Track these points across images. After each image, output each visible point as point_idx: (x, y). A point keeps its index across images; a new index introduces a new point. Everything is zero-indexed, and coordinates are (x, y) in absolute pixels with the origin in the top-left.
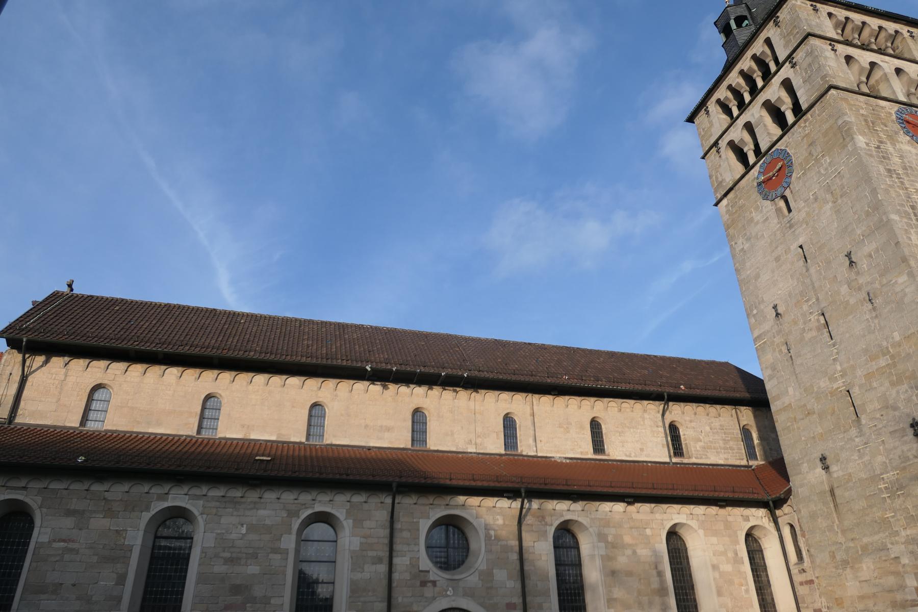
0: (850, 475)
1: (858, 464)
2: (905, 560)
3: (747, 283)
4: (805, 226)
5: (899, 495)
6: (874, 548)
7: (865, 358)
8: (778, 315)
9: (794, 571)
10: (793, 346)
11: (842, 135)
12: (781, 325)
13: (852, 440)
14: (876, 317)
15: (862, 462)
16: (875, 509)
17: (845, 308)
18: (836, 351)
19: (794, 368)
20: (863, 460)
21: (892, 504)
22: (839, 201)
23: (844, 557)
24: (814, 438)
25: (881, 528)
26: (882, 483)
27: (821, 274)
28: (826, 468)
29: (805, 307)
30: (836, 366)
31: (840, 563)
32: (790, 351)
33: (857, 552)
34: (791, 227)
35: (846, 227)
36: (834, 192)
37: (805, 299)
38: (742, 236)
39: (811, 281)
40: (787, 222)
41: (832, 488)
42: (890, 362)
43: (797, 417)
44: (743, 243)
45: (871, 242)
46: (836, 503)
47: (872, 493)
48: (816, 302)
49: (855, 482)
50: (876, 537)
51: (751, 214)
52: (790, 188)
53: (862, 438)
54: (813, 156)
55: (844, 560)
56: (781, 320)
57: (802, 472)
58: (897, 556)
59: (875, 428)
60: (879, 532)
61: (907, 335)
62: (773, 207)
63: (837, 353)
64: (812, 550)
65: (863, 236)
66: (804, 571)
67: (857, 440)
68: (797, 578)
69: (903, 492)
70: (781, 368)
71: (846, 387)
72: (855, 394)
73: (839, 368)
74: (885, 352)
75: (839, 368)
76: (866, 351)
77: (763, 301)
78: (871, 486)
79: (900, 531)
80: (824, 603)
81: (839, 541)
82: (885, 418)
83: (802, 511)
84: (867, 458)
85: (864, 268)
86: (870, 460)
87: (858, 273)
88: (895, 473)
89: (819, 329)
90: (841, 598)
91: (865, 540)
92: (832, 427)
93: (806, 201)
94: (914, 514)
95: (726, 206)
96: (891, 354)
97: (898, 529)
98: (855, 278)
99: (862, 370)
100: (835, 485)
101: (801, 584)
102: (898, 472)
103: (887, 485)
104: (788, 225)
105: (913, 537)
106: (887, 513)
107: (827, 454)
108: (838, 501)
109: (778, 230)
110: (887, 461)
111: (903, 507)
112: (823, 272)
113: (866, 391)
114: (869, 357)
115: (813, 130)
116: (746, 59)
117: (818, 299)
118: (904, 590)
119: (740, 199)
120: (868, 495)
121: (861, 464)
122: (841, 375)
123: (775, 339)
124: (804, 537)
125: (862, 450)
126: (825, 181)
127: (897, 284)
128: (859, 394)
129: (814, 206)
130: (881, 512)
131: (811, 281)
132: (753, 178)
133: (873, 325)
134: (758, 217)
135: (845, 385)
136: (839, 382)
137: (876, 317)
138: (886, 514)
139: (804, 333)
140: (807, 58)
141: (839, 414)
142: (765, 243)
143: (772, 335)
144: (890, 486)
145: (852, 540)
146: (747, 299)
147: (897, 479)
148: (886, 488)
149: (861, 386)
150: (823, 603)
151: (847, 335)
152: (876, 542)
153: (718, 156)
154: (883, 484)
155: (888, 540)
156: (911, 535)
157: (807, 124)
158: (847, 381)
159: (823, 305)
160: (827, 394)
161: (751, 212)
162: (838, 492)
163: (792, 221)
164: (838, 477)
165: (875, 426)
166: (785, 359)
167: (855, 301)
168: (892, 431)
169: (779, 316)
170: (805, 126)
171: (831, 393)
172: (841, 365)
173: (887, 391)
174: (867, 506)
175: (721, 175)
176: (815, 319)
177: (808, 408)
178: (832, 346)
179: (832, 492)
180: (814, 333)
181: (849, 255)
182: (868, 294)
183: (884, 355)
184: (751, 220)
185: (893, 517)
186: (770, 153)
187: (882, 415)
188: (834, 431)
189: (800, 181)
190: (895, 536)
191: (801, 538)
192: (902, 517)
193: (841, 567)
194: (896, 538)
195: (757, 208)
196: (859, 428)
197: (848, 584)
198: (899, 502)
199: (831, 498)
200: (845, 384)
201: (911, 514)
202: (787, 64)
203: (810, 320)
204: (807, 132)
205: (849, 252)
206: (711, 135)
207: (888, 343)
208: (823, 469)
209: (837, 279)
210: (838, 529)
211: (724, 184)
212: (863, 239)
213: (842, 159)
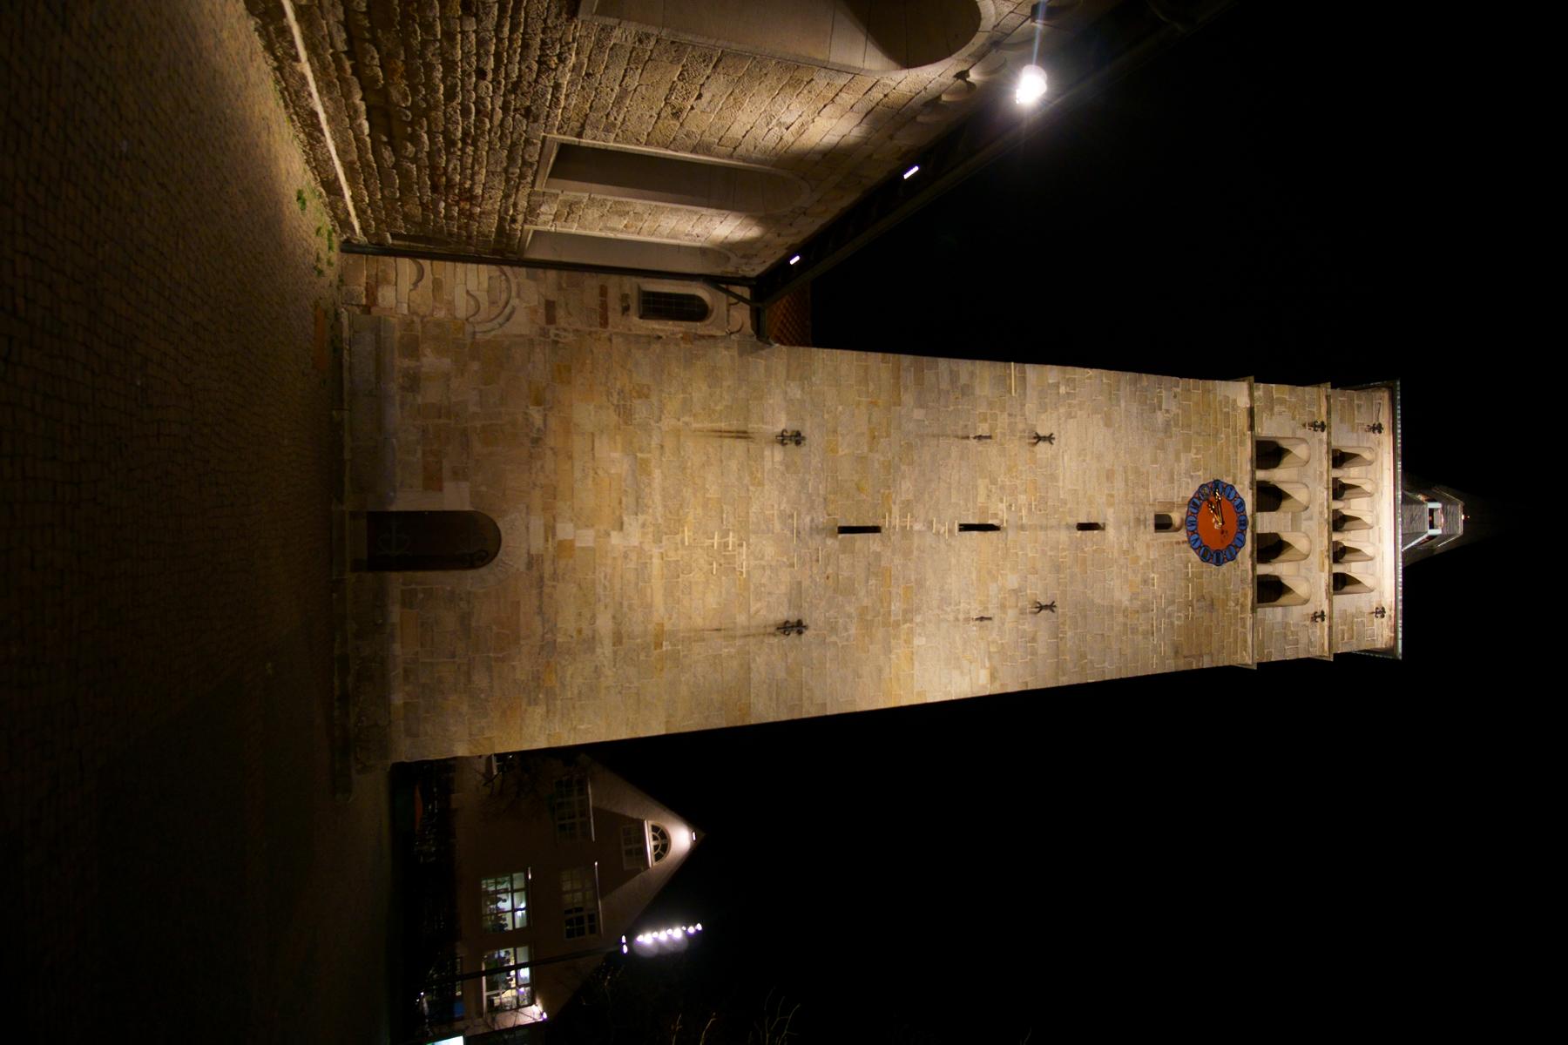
0: (761, 484)
1: (773, 506)
2: (616, 539)
3: (1110, 393)
5: (712, 564)
6: (643, 486)
7: (913, 578)
8: (1039, 438)
9: (630, 285)
10: (980, 449)
12: (1021, 438)
13: (812, 508)
14: (957, 619)
15: (773, 515)
16: (700, 511)
17: (989, 572)
18: (942, 531)
20: (776, 518)
21: (701, 547)
23: (637, 416)
24: (835, 431)
25: (670, 512)
26: (735, 540)
27: (1052, 549)
28: (783, 439)
30: (922, 524)
31: (628, 403)
32: (976, 440)
33: (641, 450)
34: (1138, 521)
35: (1085, 617)
37: (1033, 503)
38: (1178, 415)
39: (1052, 527)
41: (750, 438)
42: (892, 618)
43: (876, 409)
45: (1048, 649)
46: (725, 437)
47: (725, 516)
48: (1020, 523)
49: (748, 490)
50: (657, 498)
51: (1194, 451)
52: (1184, 542)
53: (807, 529)
55: (631, 415)
56: (1027, 441)
57: (788, 382)
58: (625, 527)
59: (814, 558)
60: (665, 506)
61: (915, 657)
62: (1180, 499)
63: (938, 533)
64: (657, 347)
65: (1062, 638)
66: (626, 310)
67: (808, 519)
68: (613, 281)
69: (714, 573)
70: (960, 407)
71: (887, 530)
72: (871, 542)
73: (917, 527)
74: (908, 614)
75: (917, 527)
76: (920, 583)
77: (1070, 416)
78: (735, 518)
79: (660, 547)
80: (565, 337)
81: (663, 417)
82: (823, 581)
83: (726, 353)
84: (777, 527)
85: (1024, 624)
86: (773, 533)
87: (1022, 612)
88: (744, 570)
89: (984, 510)
90: (569, 383)
91: (657, 473)
92: (840, 478)
93: (1153, 563)
94: (680, 580)
95: (1235, 401)
96: (901, 622)
97: (664, 542)
98: (1019, 605)
99: (899, 568)
100: (752, 446)
101: (603, 292)
102: (744, 576)
103: (730, 548)
104: (1142, 517)
105: (648, 566)
106: (691, 534)
107: (803, 449)
108: (727, 441)
109: (1148, 494)
110: (763, 563)
111: (694, 565)
112: (1052, 553)
113: (869, 564)
114: (912, 587)
117: (1022, 528)
118: (572, 520)
119: (1228, 437)
120: (725, 507)
121: (772, 512)
122: (906, 527)
123: (1006, 415)
124: (682, 338)
125: (790, 521)
126: (1157, 608)
127: (981, 668)
128: (869, 549)
129: (1139, 575)
130: (694, 521)
131: (1052, 527)
132: (1238, 481)
133: (949, 609)
136: (898, 521)
137: (957, 619)
138: (689, 531)
141: (853, 500)
142: (1143, 461)
143: (1014, 413)
144: (727, 553)
145: (662, 447)
146: (1087, 381)
147: (735, 568)
148: (726, 545)
149: (878, 556)
150: (563, 334)
151: (953, 561)
152: (650, 493)
153: (1307, 419)
154: (733, 542)
155: (650, 519)
156: (651, 563)
158: (894, 534)
159: (1011, 534)
160: (889, 488)
161: (1198, 451)
162: (740, 445)
163: (1142, 527)
164: (763, 457)
165: (818, 561)
167: (991, 593)
168: (801, 587)
169: (1035, 441)
170: (1237, 605)
172: (920, 532)
173: (857, 599)
174: (709, 499)
175: (1280, 414)
176: (998, 512)
177: (882, 440)
178: (951, 527)
179: (743, 435)
180: (981, 499)
181: (1051, 607)
182: (990, 619)
183: (905, 612)
184: (1187, 449)
185: (683, 542)
187: (828, 578)
188: (832, 477)
190: (654, 536)
191: (682, 329)
192: (679, 559)
193: (622, 402)
194: (650, 536)
195: (1196, 466)
196: (823, 529)
197: (592, 407)
198: (702, 561)
199: (734, 428)
200: (891, 530)
201: (681, 575)
203: (1002, 501)
205: (1055, 609)
207: (917, 624)
208: (783, 431)
209: (1031, 574)
210: (684, 422)
211: (1265, 415)
213: (1165, 644)
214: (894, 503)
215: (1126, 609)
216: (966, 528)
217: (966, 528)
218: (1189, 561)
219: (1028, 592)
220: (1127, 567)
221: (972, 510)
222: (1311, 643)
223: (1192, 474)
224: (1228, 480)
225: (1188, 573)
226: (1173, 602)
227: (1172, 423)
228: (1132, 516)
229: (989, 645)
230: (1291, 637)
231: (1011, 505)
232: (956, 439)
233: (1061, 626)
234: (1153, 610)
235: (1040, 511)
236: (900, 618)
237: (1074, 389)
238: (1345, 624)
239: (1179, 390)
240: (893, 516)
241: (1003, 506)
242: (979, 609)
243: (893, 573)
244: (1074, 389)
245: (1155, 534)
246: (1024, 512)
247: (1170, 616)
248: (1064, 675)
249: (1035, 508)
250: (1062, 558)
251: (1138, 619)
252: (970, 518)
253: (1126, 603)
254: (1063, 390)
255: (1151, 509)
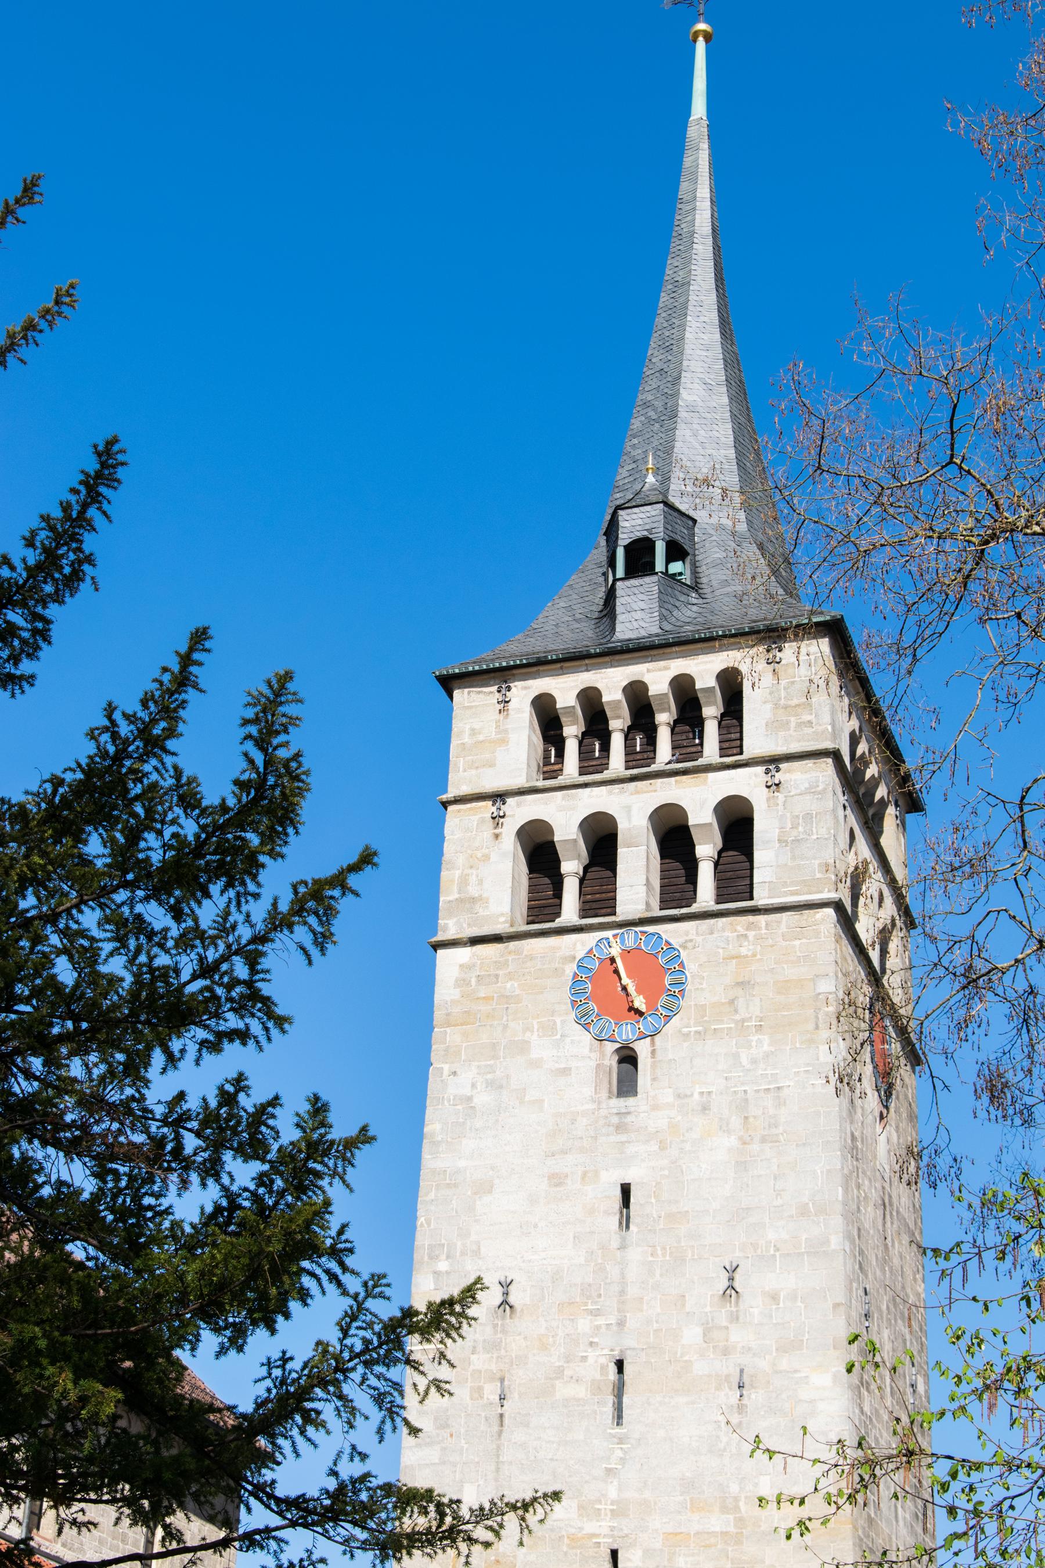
4: (654, 1147)
7: (682, 1498)
10: (516, 1395)
11: (817, 1018)
12: (504, 1332)
19: (498, 1448)
22: (755, 1147)
29: (584, 1324)
34: (620, 1128)
36: (751, 1120)
37: (590, 1307)
38: (478, 1067)
40: (615, 1111)
42: (732, 1529)
44: (474, 1086)
48: (615, 1328)
51: (528, 1034)
52: (653, 1043)
54: (736, 1011)
56: (508, 1321)
70: (462, 1430)
72: (629, 1564)
73: (613, 1493)
77: (477, 1253)
87: (735, 1318)
89: (596, 1388)
93: (679, 1096)
95: (461, 966)
98: (724, 1324)
104: (615, 1120)
112: (658, 1272)
114: (692, 1500)
115: (758, 957)
116: (667, 668)
117: (621, 1324)
119: (510, 976)
122: (612, 1511)
123: (474, 1357)
126: (743, 1084)
131: (623, 1275)
132: (568, 953)
133: (725, 1439)
134: (541, 1048)
135: (612, 1536)
136: (603, 1524)
139: (557, 1378)
140: (808, 797)
149: (648, 1553)
157: (751, 934)
159: (630, 1342)
160: (561, 1538)
163: (629, 1119)
166: (483, 1414)
171: (572, 1538)
175: (481, 882)
180: (581, 1391)
181: (732, 1271)
182: (742, 1371)
183: (724, 1509)
184: (523, 1047)
186: (638, 929)
189: (686, 1044)
195: (549, 1029)
200: (615, 1533)
202: (760, 769)
203: (584, 1359)
204: (744, 951)
206: (491, 764)
209: (684, 1305)
212: (774, 1256)
214: (581, 1529)
215: (740, 1138)
216: (619, 1416)
217: (619, 1416)
218: (680, 1031)
219: (708, 1309)
220: (683, 1141)
221: (596, 1407)
222: (811, 787)
223: (558, 1037)
224: (571, 968)
225: (696, 1032)
226: (736, 1056)
227: (489, 1076)
228: (613, 1138)
229: (776, 1372)
230: (801, 829)
231: (591, 1344)
232: (504, 1434)
233: (759, 1252)
234: (745, 1091)
235: (600, 1296)
236: (731, 1517)
237: (443, 1245)
238: (788, 722)
239: (446, 1068)
240: (597, 1532)
241: (592, 1354)
242: (727, 1389)
243: (671, 1531)
244: (443, 1245)
245: (639, 1096)
246: (601, 1321)
247: (754, 1061)
248: (827, 1242)
249: (596, 1303)
250: (664, 1255)
251: (755, 1117)
252: (605, 1409)
253: (733, 1141)
254: (443, 1266)
255: (604, 1105)
